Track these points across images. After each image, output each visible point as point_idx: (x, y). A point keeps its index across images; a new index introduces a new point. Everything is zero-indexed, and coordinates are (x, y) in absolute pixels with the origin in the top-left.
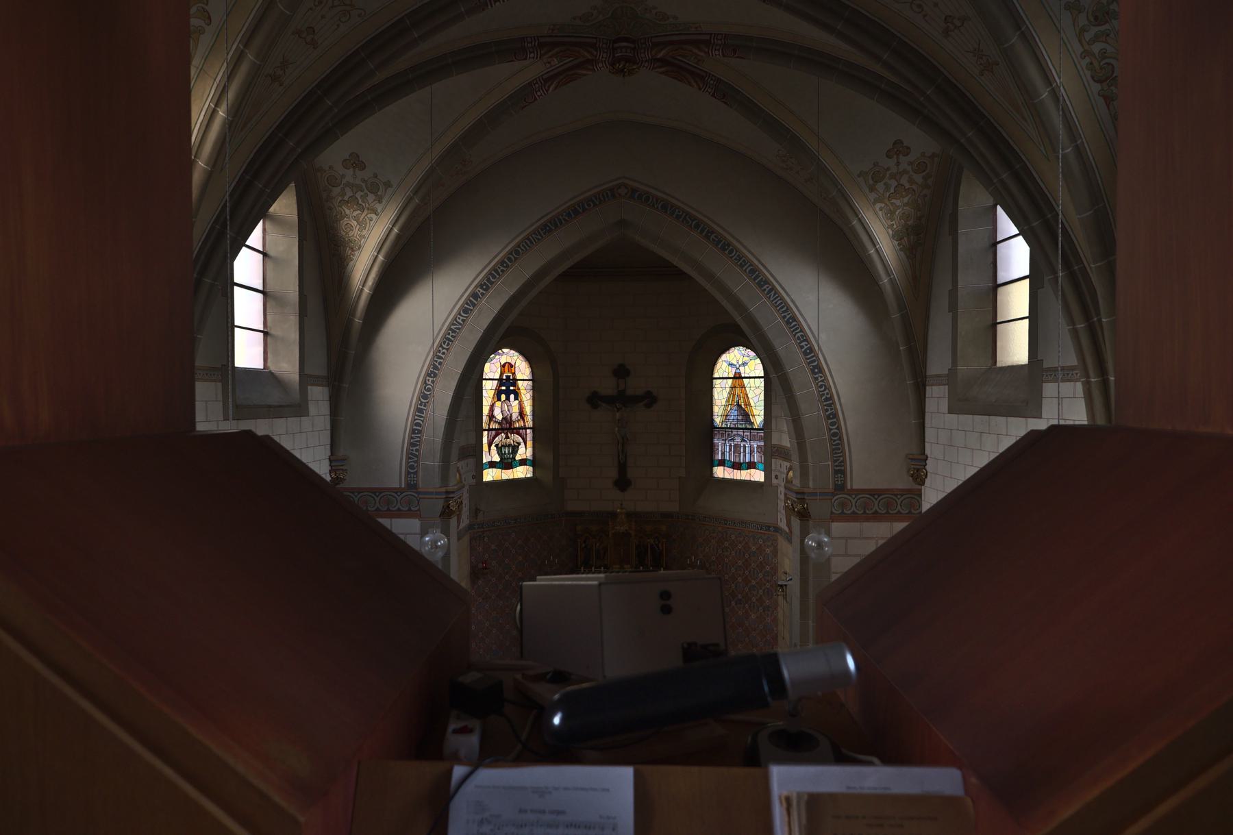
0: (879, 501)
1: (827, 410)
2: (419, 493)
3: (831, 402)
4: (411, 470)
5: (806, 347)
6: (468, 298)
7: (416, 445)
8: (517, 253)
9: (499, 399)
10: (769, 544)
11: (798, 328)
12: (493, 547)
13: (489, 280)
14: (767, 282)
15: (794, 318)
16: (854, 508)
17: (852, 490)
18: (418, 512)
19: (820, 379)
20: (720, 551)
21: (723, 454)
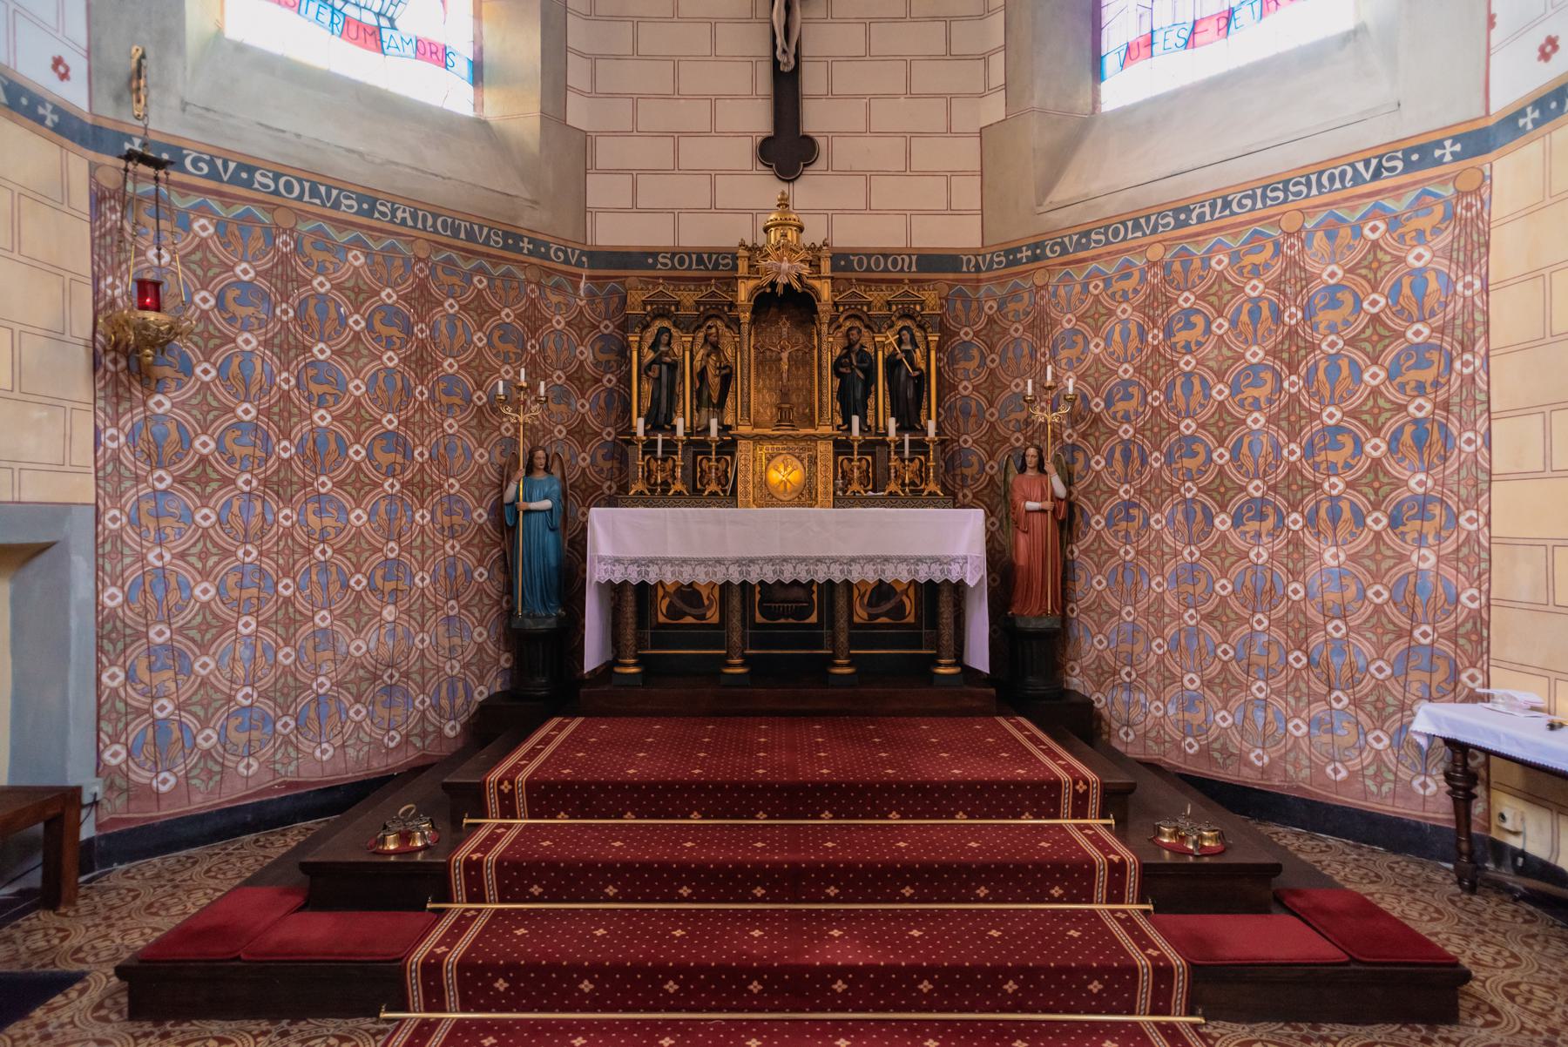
20: (1155, 336)
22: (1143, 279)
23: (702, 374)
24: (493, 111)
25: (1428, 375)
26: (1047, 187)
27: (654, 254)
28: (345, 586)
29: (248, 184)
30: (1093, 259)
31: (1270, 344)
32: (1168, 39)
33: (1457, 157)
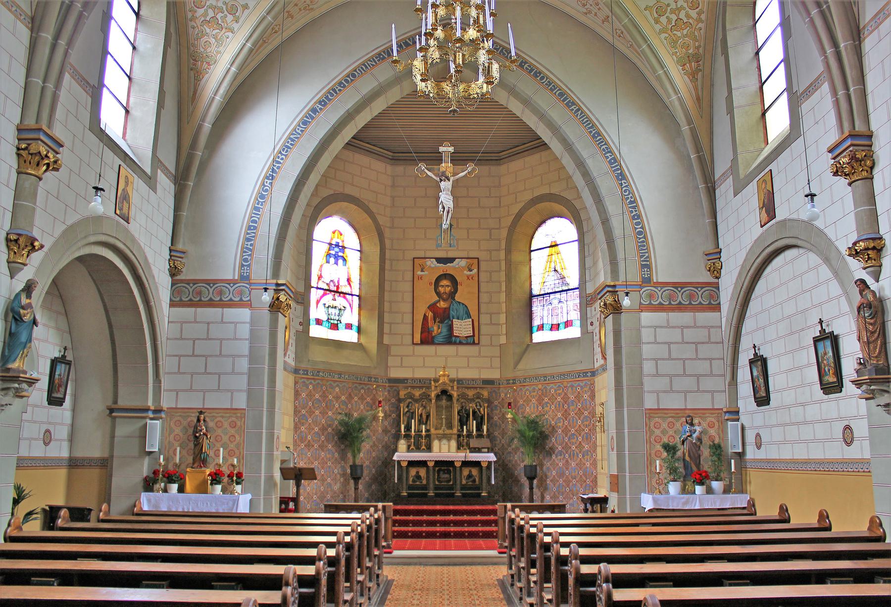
0: (682, 294)
1: (632, 212)
2: (250, 284)
3: (635, 204)
4: (245, 263)
5: (610, 158)
6: (307, 112)
7: (252, 240)
8: (354, 76)
9: (328, 262)
10: (587, 389)
11: (602, 142)
12: (317, 396)
13: (327, 97)
14: (574, 103)
15: (599, 134)
16: (660, 300)
17: (658, 283)
18: (250, 302)
19: (624, 185)
21: (542, 318)
22: (538, 393)
23: (421, 415)
24: (362, 341)
25: (587, 423)
26: (517, 363)
27: (407, 379)
28: (333, 472)
29: (318, 376)
30: (527, 385)
31: (562, 413)
32: (547, 327)
33: (591, 376)
